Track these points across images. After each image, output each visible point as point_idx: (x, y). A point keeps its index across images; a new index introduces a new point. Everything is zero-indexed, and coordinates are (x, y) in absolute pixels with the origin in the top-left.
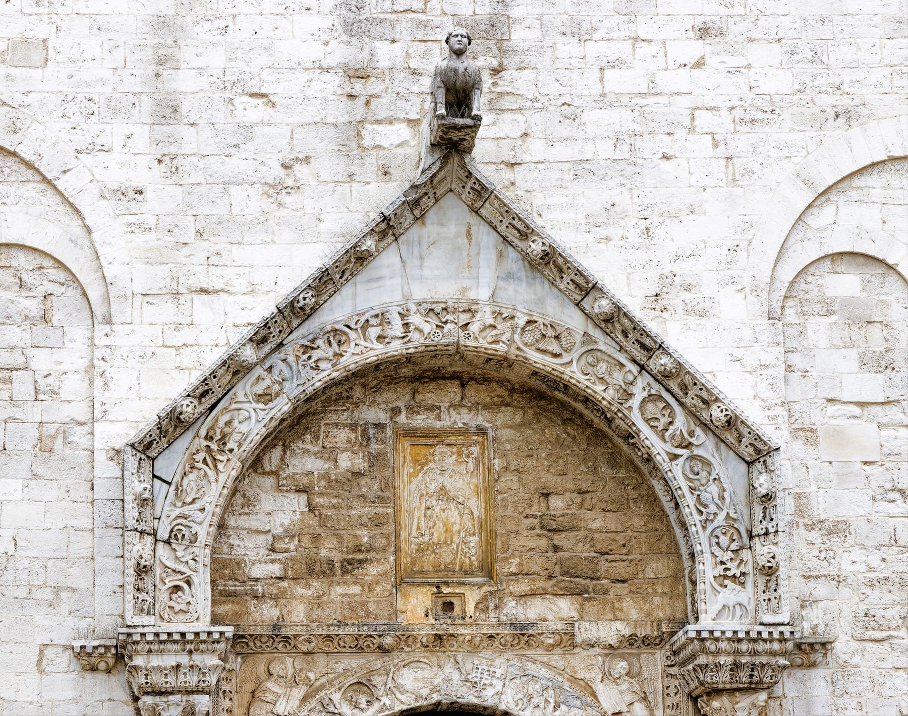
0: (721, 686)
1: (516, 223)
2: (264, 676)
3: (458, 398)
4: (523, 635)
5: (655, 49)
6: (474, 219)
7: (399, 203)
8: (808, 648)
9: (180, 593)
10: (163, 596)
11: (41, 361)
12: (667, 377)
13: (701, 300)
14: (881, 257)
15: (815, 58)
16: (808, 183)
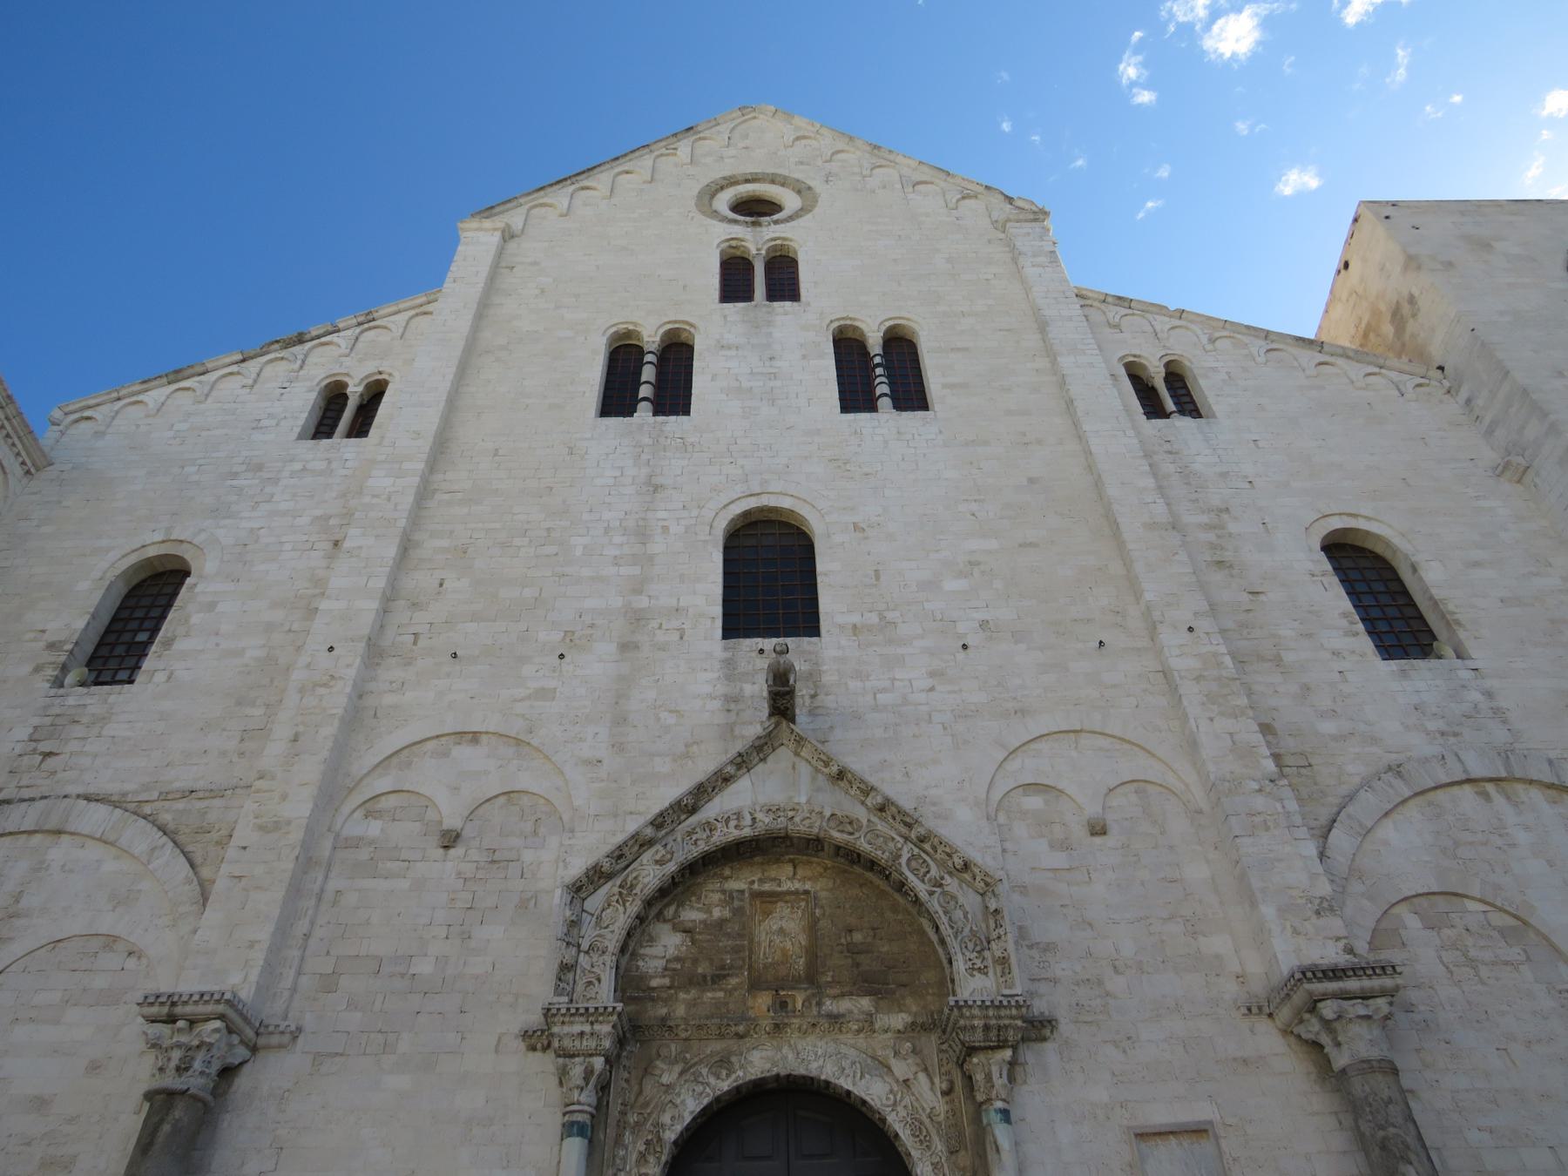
0: (977, 1044)
1: (822, 756)
3: (791, 874)
4: (836, 1023)
6: (797, 760)
8: (1039, 1025)
9: (592, 987)
10: (580, 987)
12: (922, 841)
14: (1053, 785)
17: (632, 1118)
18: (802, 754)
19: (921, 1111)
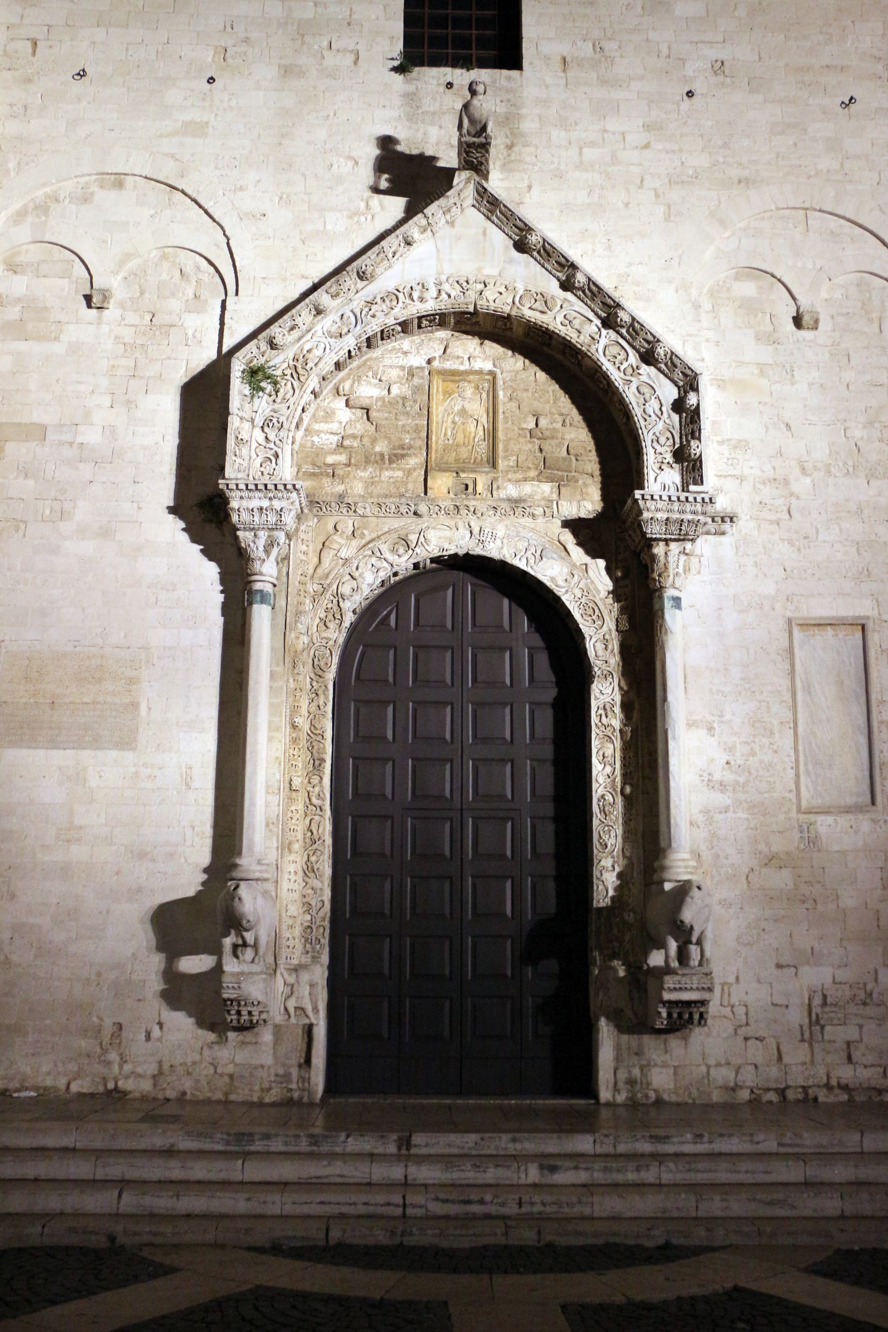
2: (332, 531)
15: (725, 145)
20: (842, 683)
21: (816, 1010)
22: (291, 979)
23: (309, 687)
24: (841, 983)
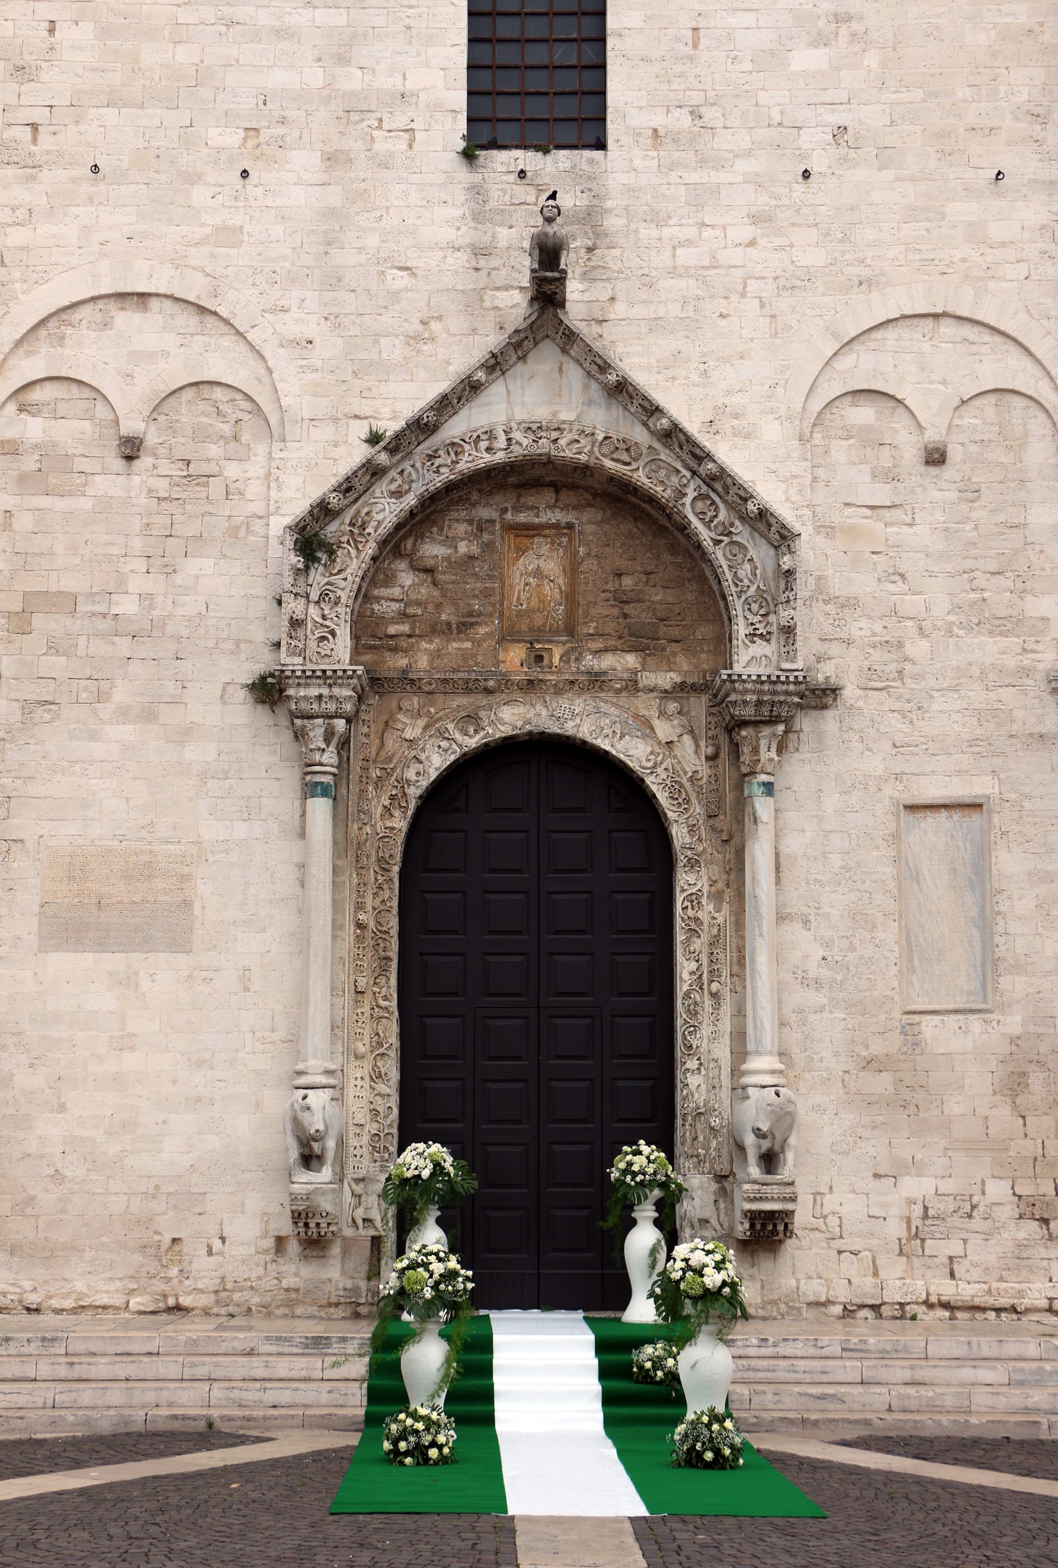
1: (597, 360)
3: (553, 501)
5: (717, 232)
6: (565, 359)
7: (504, 344)
10: (312, 644)
11: (232, 470)
12: (713, 479)
13: (746, 426)
15: (845, 239)
16: (836, 335)
17: (374, 773)
18: (571, 352)
19: (681, 773)
20: (955, 870)
21: (916, 1222)
22: (359, 1189)
23: (373, 880)
24: (944, 1195)
